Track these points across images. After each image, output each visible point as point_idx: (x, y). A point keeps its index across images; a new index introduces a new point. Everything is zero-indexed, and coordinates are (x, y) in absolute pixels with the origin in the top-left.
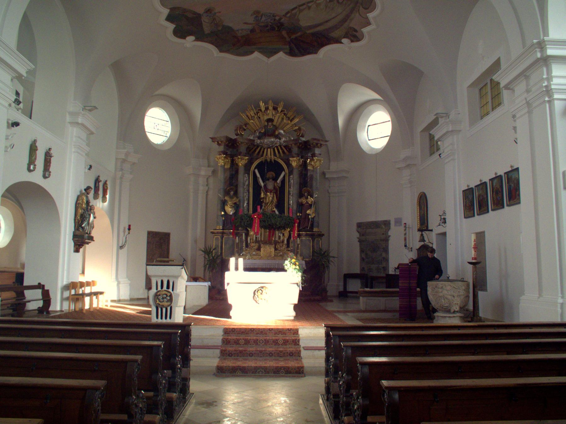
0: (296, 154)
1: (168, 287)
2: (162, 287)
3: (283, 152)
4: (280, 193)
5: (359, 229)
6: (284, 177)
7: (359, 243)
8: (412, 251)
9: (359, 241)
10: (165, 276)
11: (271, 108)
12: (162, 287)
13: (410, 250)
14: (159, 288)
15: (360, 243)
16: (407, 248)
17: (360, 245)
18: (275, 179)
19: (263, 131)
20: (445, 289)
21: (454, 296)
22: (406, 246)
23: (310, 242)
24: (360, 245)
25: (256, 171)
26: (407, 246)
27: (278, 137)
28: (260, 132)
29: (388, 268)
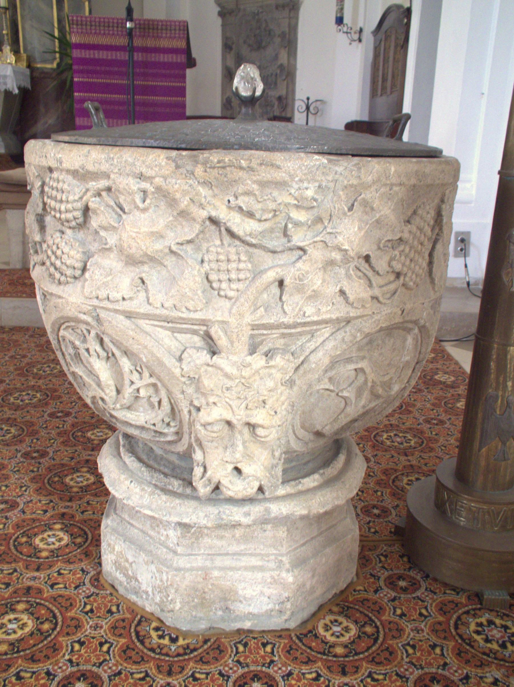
7: (219, 21)
8: (360, 40)
9: (221, 14)
13: (356, 37)
15: (223, 21)
16: (345, 29)
17: (224, 26)
20: (112, 240)
21: (216, 331)
22: (340, 21)
23: (52, 8)
24: (223, 25)
26: (345, 21)
29: (294, 100)
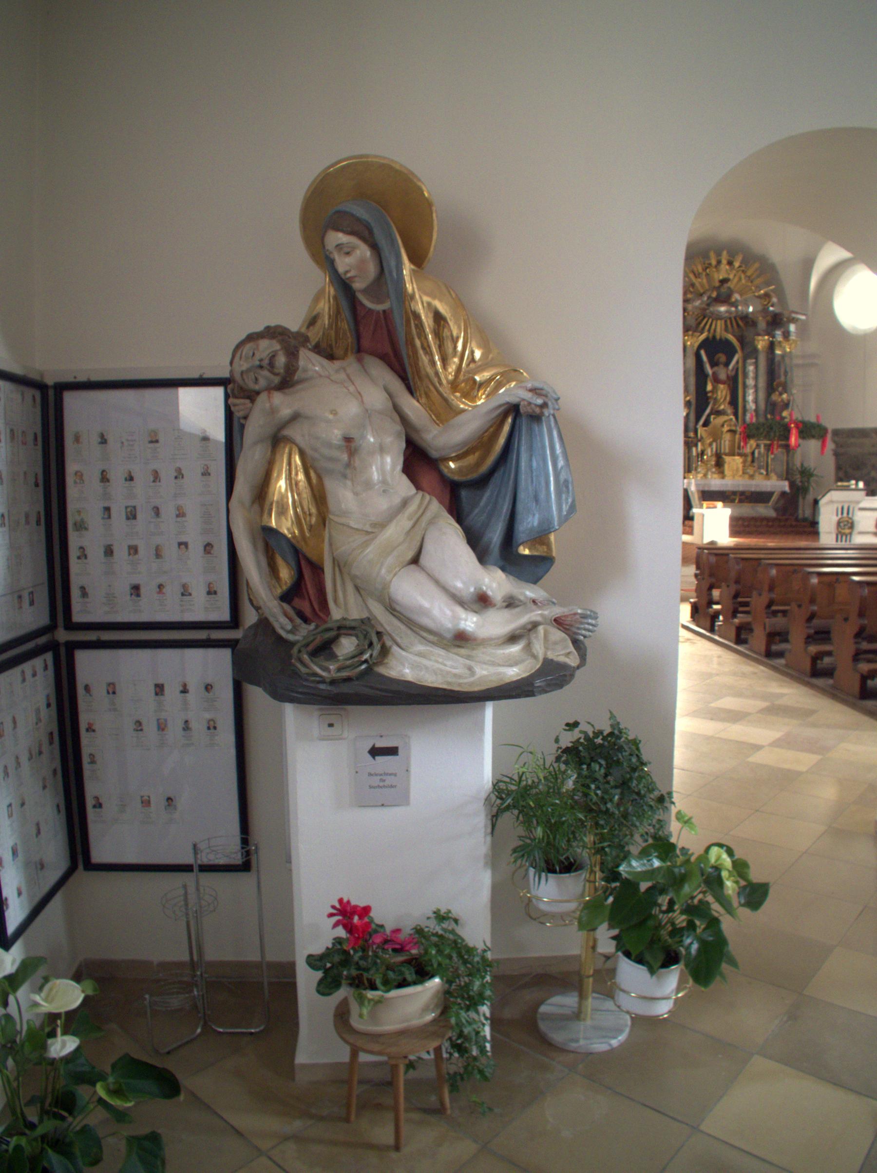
0: (763, 331)
1: (848, 513)
2: (842, 513)
3: (738, 325)
4: (733, 383)
5: (836, 439)
6: (737, 362)
10: (844, 502)
11: (724, 262)
12: (842, 513)
14: (840, 516)
18: (727, 365)
19: (714, 295)
25: (703, 352)
27: (735, 304)
28: (709, 297)
